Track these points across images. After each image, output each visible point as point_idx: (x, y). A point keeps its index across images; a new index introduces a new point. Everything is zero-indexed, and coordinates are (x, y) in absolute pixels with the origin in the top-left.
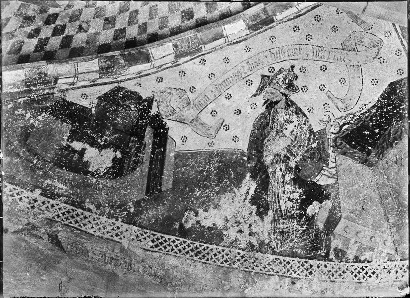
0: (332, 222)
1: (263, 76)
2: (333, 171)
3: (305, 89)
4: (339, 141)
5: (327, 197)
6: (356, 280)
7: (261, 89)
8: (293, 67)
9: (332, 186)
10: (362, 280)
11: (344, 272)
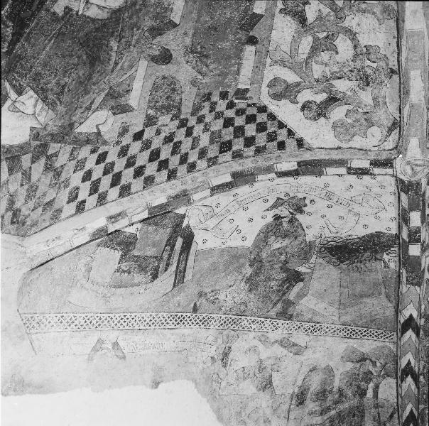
0: (300, 296)
1: (278, 199)
2: (312, 266)
3: (309, 214)
4: (323, 249)
5: (302, 280)
7: (274, 206)
8: (305, 198)
9: (308, 273)
11: (299, 328)
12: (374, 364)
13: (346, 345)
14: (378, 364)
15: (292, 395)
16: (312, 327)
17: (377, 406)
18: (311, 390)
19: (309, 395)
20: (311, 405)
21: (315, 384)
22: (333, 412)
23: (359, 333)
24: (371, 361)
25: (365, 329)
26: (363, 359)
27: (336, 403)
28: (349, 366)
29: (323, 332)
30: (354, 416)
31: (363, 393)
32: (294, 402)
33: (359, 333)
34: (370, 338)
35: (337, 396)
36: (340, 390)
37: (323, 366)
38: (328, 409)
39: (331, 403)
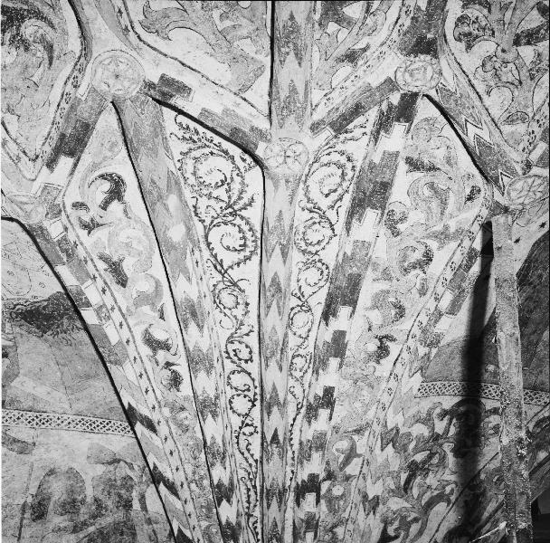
4: (14, 315)
6: (29, 425)
9: (10, 347)
10: (35, 426)
12: (131, 466)
13: (89, 441)
14: (136, 467)
15: (24, 505)
16: (37, 417)
17: (149, 521)
18: (53, 499)
19: (51, 507)
20: (57, 520)
21: (58, 490)
22: (92, 529)
24: (126, 462)
26: (115, 461)
27: (94, 517)
28: (100, 469)
29: (53, 425)
30: (122, 534)
31: (127, 505)
32: (27, 515)
35: (94, 507)
37: (64, 469)
38: (85, 524)
39: (86, 517)
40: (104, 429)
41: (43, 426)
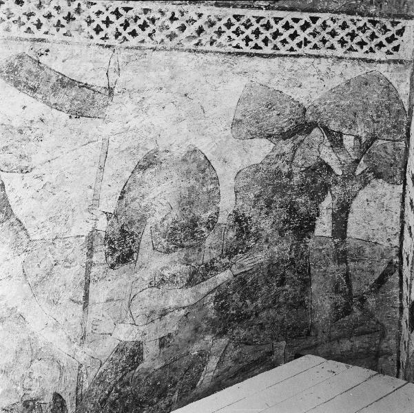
6: (97, 38)
10: (112, 41)
11: (69, 18)
12: (336, 141)
13: (246, 81)
14: (349, 142)
15: (91, 239)
16: (117, 14)
17: (342, 257)
18: (151, 221)
19: (146, 238)
20: (155, 261)
21: (160, 199)
22: (223, 276)
23: (286, 34)
24: (327, 130)
25: (306, 17)
26: (301, 127)
27: (230, 253)
28: (261, 150)
29: (159, 36)
30: (282, 282)
31: (305, 226)
32: (99, 257)
33: (286, 34)
34: (322, 52)
35: (231, 234)
36: (239, 220)
37: (178, 152)
38: (210, 268)
39: (215, 253)
40: (293, 44)
41: (133, 41)
